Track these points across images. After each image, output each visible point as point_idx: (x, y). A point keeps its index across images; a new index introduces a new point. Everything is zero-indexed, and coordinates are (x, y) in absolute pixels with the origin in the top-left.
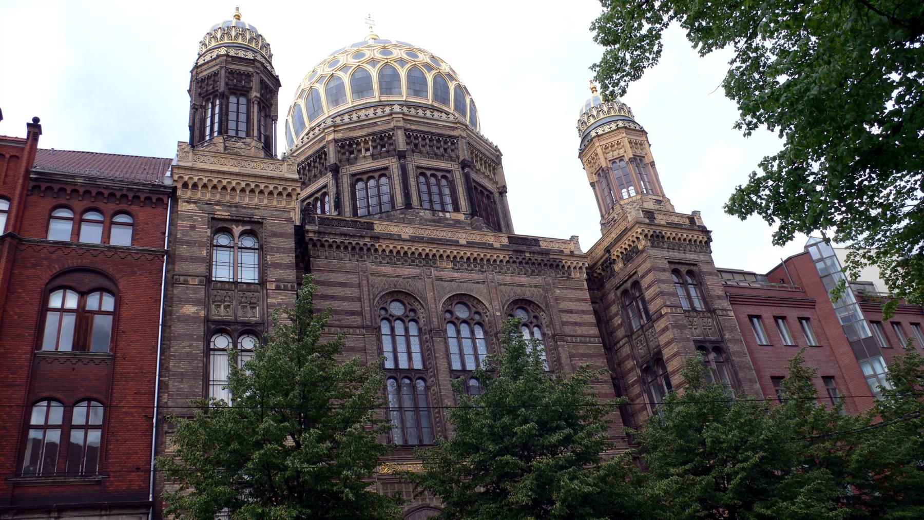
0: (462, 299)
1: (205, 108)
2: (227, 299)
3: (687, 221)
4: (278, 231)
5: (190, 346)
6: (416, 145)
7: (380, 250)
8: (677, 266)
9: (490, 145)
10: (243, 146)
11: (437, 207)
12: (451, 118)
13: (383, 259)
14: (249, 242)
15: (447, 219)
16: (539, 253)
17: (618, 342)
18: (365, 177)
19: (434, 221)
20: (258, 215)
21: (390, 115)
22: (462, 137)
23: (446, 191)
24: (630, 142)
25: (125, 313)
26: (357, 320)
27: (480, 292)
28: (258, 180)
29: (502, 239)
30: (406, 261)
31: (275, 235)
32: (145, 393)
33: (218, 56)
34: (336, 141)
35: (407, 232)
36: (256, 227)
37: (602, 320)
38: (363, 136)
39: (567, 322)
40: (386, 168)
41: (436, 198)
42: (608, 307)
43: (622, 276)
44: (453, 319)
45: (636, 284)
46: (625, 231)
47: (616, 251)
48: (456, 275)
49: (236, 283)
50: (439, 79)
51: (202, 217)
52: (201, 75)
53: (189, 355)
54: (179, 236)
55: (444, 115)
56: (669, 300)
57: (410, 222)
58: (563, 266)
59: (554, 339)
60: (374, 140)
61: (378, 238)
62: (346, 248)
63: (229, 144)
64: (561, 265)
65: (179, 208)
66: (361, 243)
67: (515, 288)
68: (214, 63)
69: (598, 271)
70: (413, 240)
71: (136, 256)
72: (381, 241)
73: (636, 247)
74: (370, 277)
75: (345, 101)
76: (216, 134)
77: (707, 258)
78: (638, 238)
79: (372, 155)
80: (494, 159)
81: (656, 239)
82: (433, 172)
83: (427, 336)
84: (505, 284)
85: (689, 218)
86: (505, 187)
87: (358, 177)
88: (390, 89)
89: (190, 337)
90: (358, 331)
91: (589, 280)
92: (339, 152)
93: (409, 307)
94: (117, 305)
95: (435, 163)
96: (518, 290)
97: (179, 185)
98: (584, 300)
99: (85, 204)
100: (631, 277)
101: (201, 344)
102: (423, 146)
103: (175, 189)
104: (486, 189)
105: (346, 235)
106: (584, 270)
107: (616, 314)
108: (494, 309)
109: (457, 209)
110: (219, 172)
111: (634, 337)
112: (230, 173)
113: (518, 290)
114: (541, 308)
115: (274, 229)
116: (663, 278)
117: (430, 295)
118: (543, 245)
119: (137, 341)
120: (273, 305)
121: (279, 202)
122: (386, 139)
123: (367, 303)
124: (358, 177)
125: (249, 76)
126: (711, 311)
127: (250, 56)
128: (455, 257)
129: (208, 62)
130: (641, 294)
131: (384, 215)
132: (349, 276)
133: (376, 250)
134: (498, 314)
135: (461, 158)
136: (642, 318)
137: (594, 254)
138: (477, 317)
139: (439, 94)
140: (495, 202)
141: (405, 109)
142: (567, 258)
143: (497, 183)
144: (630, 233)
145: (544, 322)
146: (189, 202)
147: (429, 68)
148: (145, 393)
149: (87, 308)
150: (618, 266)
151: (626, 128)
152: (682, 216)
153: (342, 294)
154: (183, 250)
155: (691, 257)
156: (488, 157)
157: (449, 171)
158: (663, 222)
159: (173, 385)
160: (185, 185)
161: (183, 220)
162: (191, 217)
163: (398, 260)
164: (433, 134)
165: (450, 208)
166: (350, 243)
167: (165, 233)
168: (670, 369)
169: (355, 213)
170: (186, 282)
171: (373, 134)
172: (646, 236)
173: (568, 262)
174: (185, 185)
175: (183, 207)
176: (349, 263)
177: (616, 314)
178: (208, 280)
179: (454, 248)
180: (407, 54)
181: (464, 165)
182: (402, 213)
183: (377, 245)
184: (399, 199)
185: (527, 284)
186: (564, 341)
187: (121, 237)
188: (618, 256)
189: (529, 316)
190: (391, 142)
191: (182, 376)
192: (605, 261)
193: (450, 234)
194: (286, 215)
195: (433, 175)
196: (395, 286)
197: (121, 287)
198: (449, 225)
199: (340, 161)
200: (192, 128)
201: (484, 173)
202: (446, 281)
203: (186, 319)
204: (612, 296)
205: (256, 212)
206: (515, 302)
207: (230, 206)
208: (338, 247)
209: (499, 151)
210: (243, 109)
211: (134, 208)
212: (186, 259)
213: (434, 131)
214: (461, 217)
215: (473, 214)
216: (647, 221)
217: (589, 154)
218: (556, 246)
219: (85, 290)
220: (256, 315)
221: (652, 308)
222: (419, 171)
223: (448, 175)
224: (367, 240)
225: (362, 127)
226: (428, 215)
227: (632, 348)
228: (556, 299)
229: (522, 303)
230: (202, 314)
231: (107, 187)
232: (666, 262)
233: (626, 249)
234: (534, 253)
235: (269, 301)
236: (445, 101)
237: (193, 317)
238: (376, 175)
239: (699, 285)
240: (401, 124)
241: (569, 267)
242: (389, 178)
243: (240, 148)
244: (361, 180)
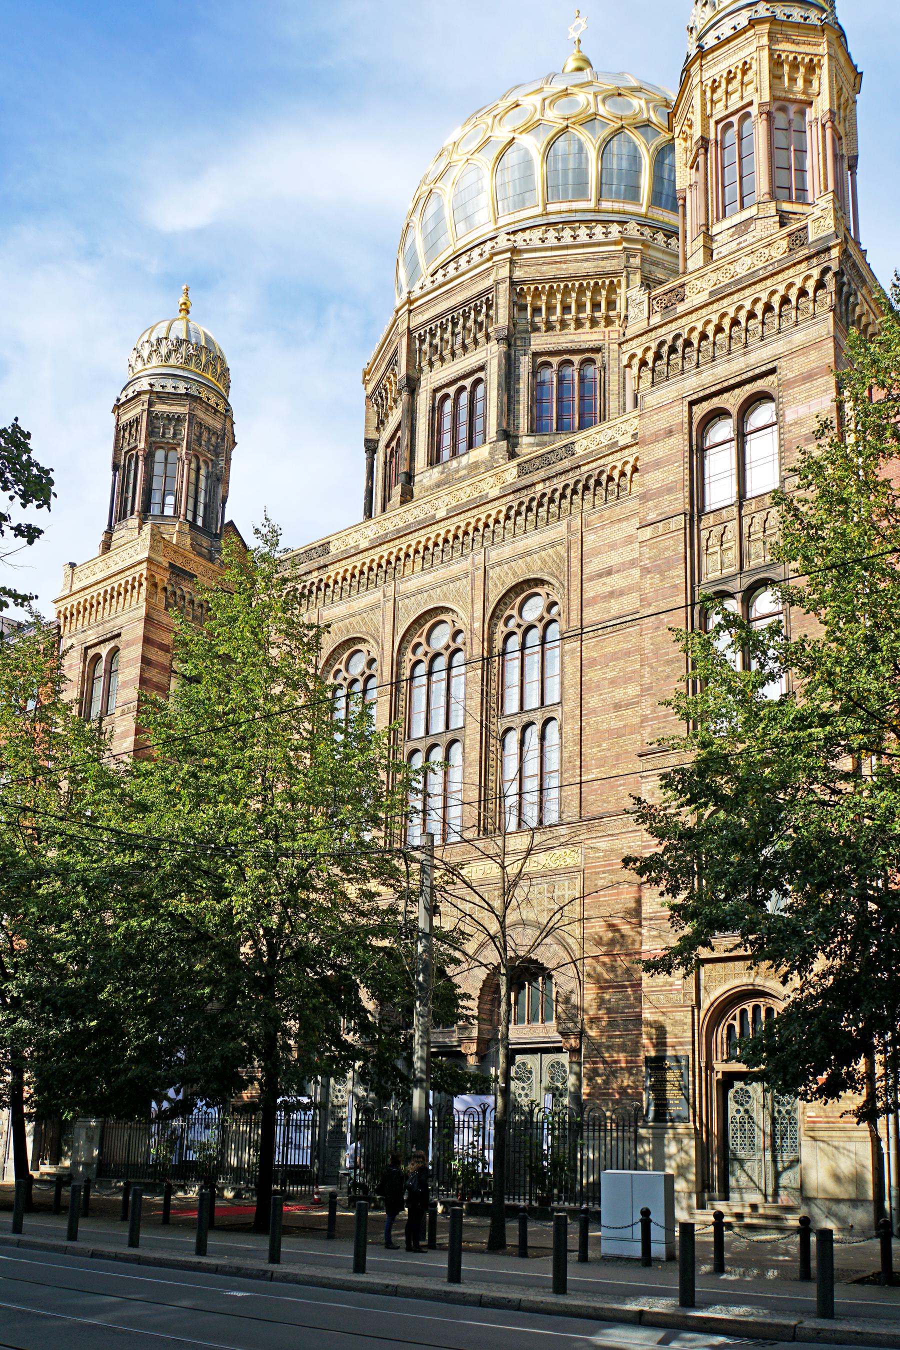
39: (594, 598)
48: (428, 578)
58: (610, 479)
164: (453, 309)
198: (463, 479)
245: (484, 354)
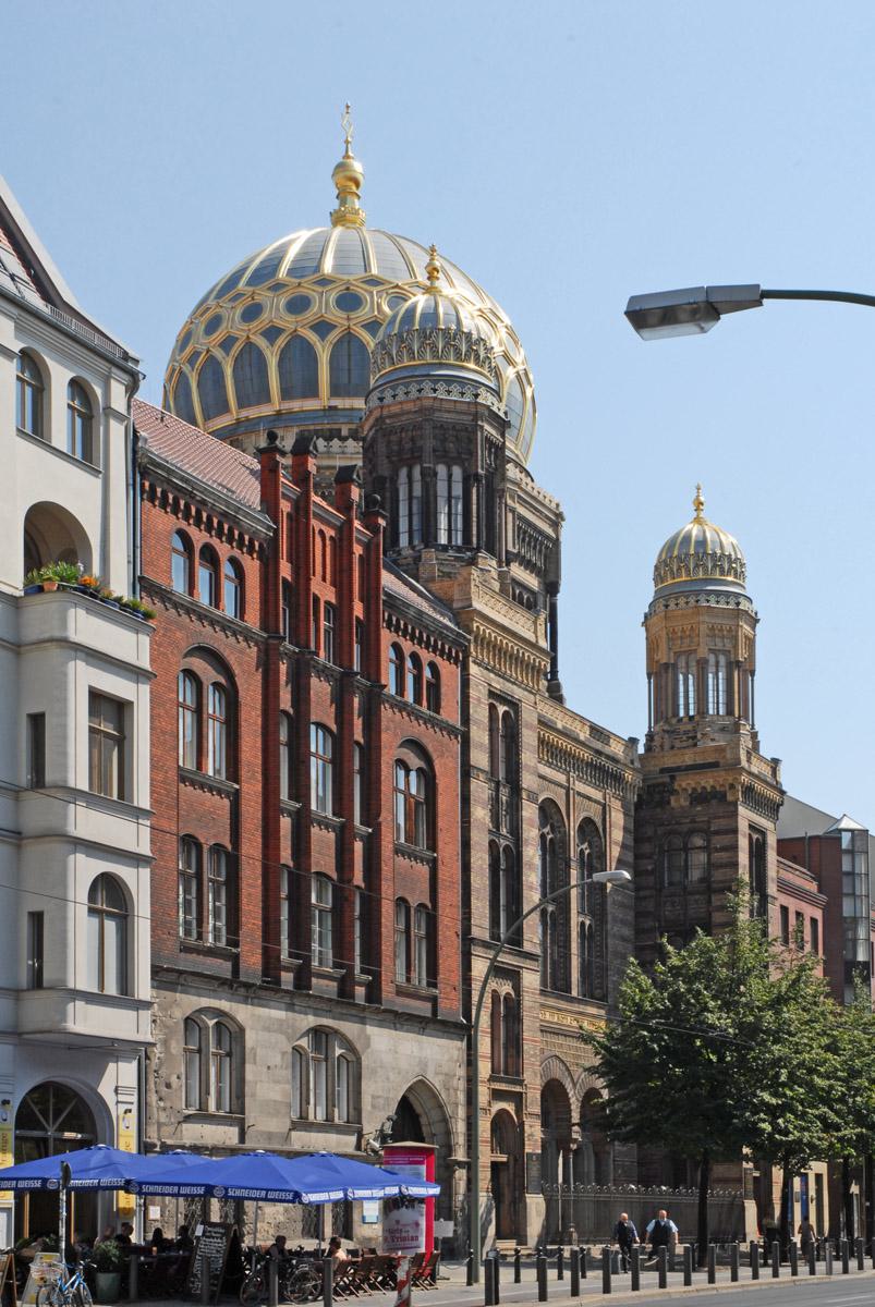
47: (686, 783)
73: (724, 795)
78: (732, 786)
146: (474, 662)
150: (679, 802)
160: (476, 638)
175: (474, 669)
188: (685, 790)
211: (438, 660)
233: (704, 788)
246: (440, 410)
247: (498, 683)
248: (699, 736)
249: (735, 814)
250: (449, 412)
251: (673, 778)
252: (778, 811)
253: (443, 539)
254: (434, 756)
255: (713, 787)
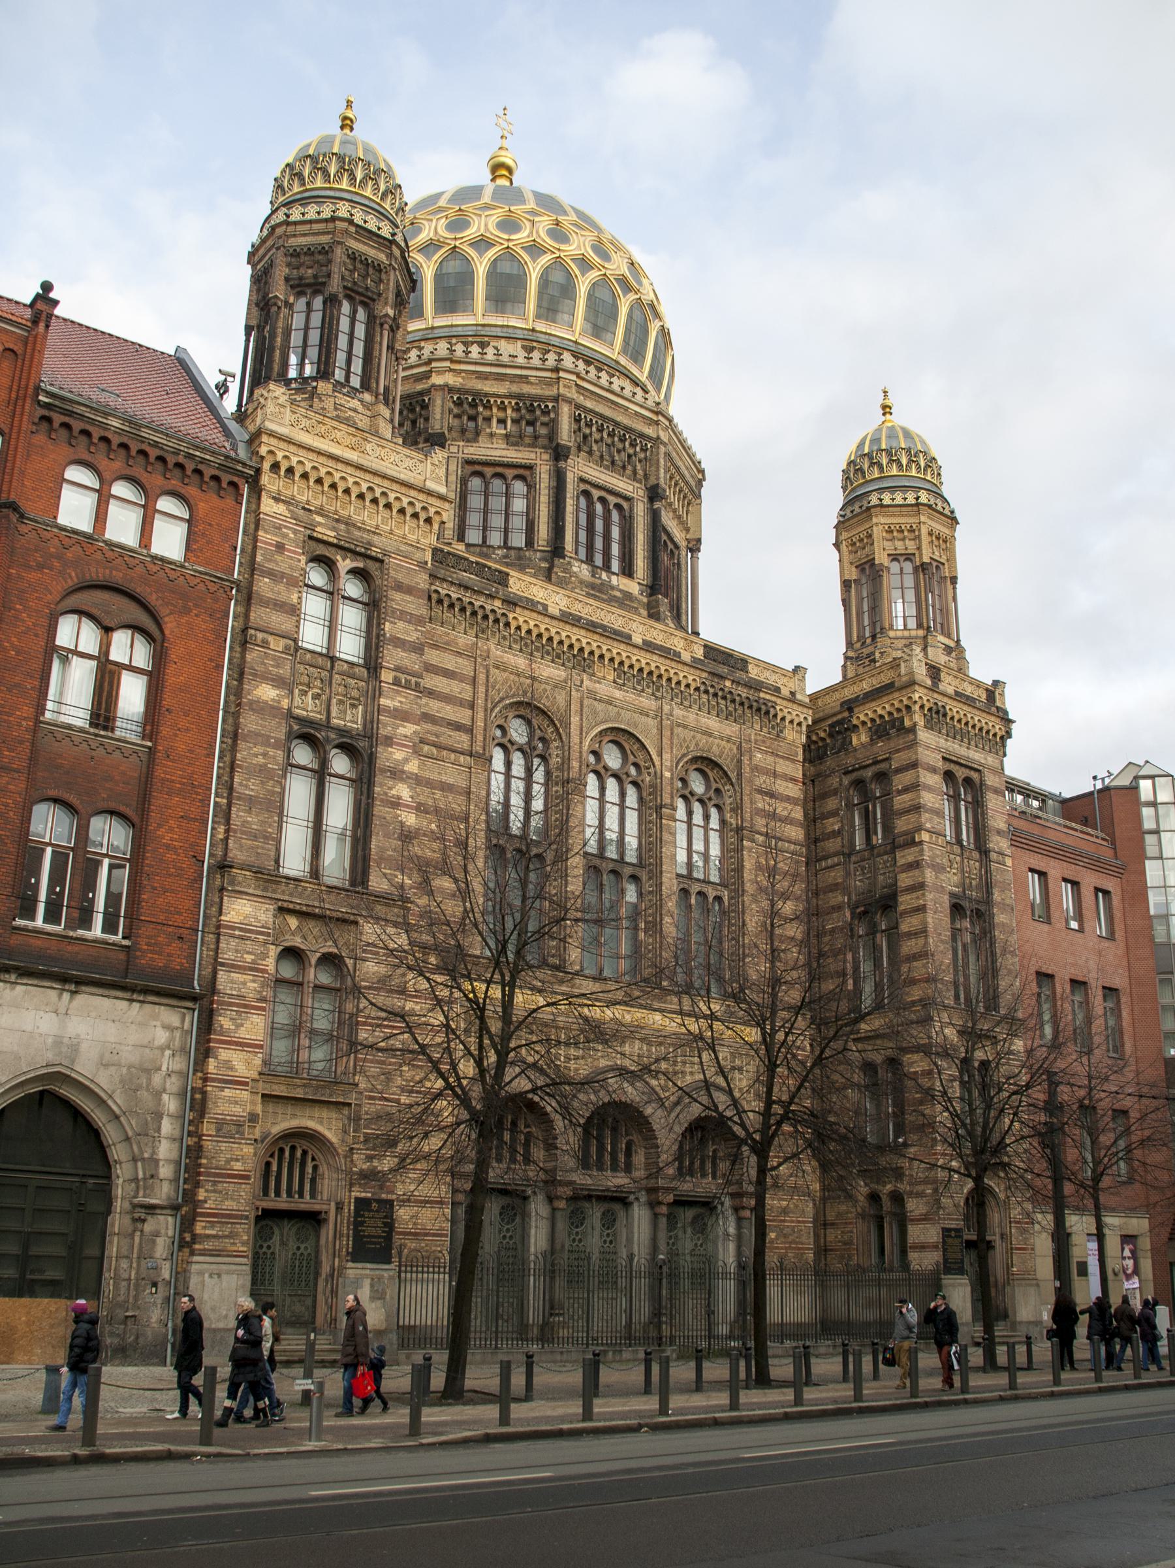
0: (620, 737)
1: (290, 306)
2: (318, 683)
3: (984, 697)
4: (406, 581)
5: (265, 755)
6: (585, 437)
7: (514, 625)
8: (952, 767)
9: (691, 456)
10: (360, 408)
11: (599, 560)
12: (650, 403)
13: (515, 641)
14: (353, 588)
15: (613, 588)
16: (746, 686)
17: (826, 858)
18: (489, 471)
19: (592, 586)
20: (379, 545)
21: (556, 370)
22: (663, 443)
23: (615, 532)
24: (930, 534)
25: (173, 677)
26: (461, 740)
27: (646, 730)
28: (386, 483)
29: (695, 647)
30: (548, 653)
31: (399, 587)
32: (195, 820)
33: (333, 219)
34: (451, 390)
35: (556, 600)
36: (372, 566)
37: (812, 821)
38: (499, 396)
40: (530, 468)
41: (599, 543)
42: (824, 796)
43: (863, 757)
44: (599, 768)
45: (882, 777)
46: (888, 688)
48: (618, 694)
49: (333, 659)
50: (637, 314)
51: (295, 532)
52: (292, 242)
53: (263, 769)
54: (259, 558)
55: (638, 390)
56: (931, 820)
57: (562, 584)
58: (775, 716)
59: (735, 835)
60: (517, 409)
61: (515, 605)
62: (463, 610)
63: (342, 399)
64: (772, 711)
65: (263, 508)
66: (489, 608)
67: (699, 735)
68: (322, 226)
69: (822, 735)
70: (567, 618)
71: (194, 582)
72: (518, 610)
73: (902, 720)
74: (492, 670)
75: (469, 309)
76: (308, 371)
77: (997, 764)
78: (908, 708)
79: (507, 436)
80: (693, 484)
81: (936, 716)
82: (603, 494)
83: (559, 788)
84: (685, 727)
85: (987, 690)
86: (699, 541)
87: (478, 468)
88: (555, 311)
89: (265, 741)
90: (462, 758)
91: (807, 748)
92: (450, 411)
93: (538, 733)
94: (160, 657)
95: (609, 479)
96: (703, 740)
97: (266, 466)
98: (793, 780)
99: (118, 465)
100: (876, 763)
101: (280, 755)
102: (596, 442)
103: (258, 471)
104: (671, 540)
105: (466, 588)
106: (804, 728)
107: (834, 813)
108: (666, 765)
109: (628, 570)
110: (331, 457)
111: (853, 858)
112: (347, 463)
113: (703, 740)
114: (729, 779)
115: (400, 577)
116: (931, 783)
117: (575, 720)
118: (754, 672)
119: (188, 730)
120: (387, 710)
121: (412, 530)
122: (538, 413)
123: (480, 715)
124: (478, 468)
125: (379, 269)
126: (983, 850)
127: (386, 231)
128: (621, 663)
129: (311, 222)
130: (887, 793)
131: (512, 553)
132: (460, 660)
133: (507, 624)
134: (667, 774)
135: (652, 481)
136: (876, 834)
137: (820, 703)
138: (633, 771)
139: (632, 343)
140: (679, 564)
141: (581, 365)
142: (785, 703)
143: (688, 530)
144: (896, 695)
145: (729, 801)
146: (277, 500)
147: (627, 287)
148: (195, 820)
149: (112, 657)
150: (860, 739)
151: (930, 506)
152: (978, 684)
153: (446, 691)
154: (264, 586)
155: (976, 756)
156: (687, 483)
157: (628, 499)
158: (950, 690)
159: (239, 815)
160: (275, 467)
161: (266, 532)
162: (279, 528)
163: (537, 649)
164: (617, 424)
165: (615, 566)
166: (471, 603)
167: (236, 548)
168: (904, 927)
169: (461, 538)
170: (265, 644)
171: (519, 397)
172: (922, 707)
173: (784, 709)
174: (275, 467)
175: (268, 505)
176: (465, 640)
177: (834, 813)
178: (295, 648)
179: (623, 646)
180: (594, 248)
181: (654, 494)
182: (542, 559)
183: (511, 616)
184: (543, 531)
185: (716, 731)
186: (753, 841)
187: (170, 541)
188: (864, 723)
189: (708, 787)
190: (545, 419)
191: (251, 802)
192: (840, 722)
193: (621, 621)
194: (418, 555)
195: (602, 500)
196: (525, 693)
197: (167, 632)
198: (612, 600)
199: (450, 429)
200: (248, 329)
201: (675, 511)
202: (600, 701)
203: (262, 708)
204: (834, 781)
205: (376, 539)
206: (695, 760)
207: (338, 521)
208: (452, 606)
209: (702, 472)
210: (360, 330)
211: (192, 491)
212: (266, 603)
213: (619, 418)
214: (633, 587)
215: (653, 588)
216: (929, 682)
217: (859, 531)
218: (771, 679)
219: (112, 625)
220: (351, 719)
221: (902, 825)
222: (583, 487)
223: (625, 505)
224: (498, 603)
225: (500, 378)
226: (582, 571)
227: (848, 874)
228: (756, 769)
229: (705, 764)
230: (285, 703)
231: (156, 445)
232: (939, 757)
233: (881, 717)
234: (738, 683)
235: (383, 701)
236: (637, 356)
237: (272, 707)
238: (510, 473)
239: (978, 805)
240: (573, 394)
241: (783, 719)
242: (531, 487)
243: (355, 411)
244: (480, 474)
245: (631, 488)
246: (295, 236)
247: (334, 529)
248: (877, 655)
249: (914, 744)
250: (305, 235)
251: (850, 710)
252: (1004, 746)
253: (292, 373)
254: (163, 611)
255: (890, 714)
